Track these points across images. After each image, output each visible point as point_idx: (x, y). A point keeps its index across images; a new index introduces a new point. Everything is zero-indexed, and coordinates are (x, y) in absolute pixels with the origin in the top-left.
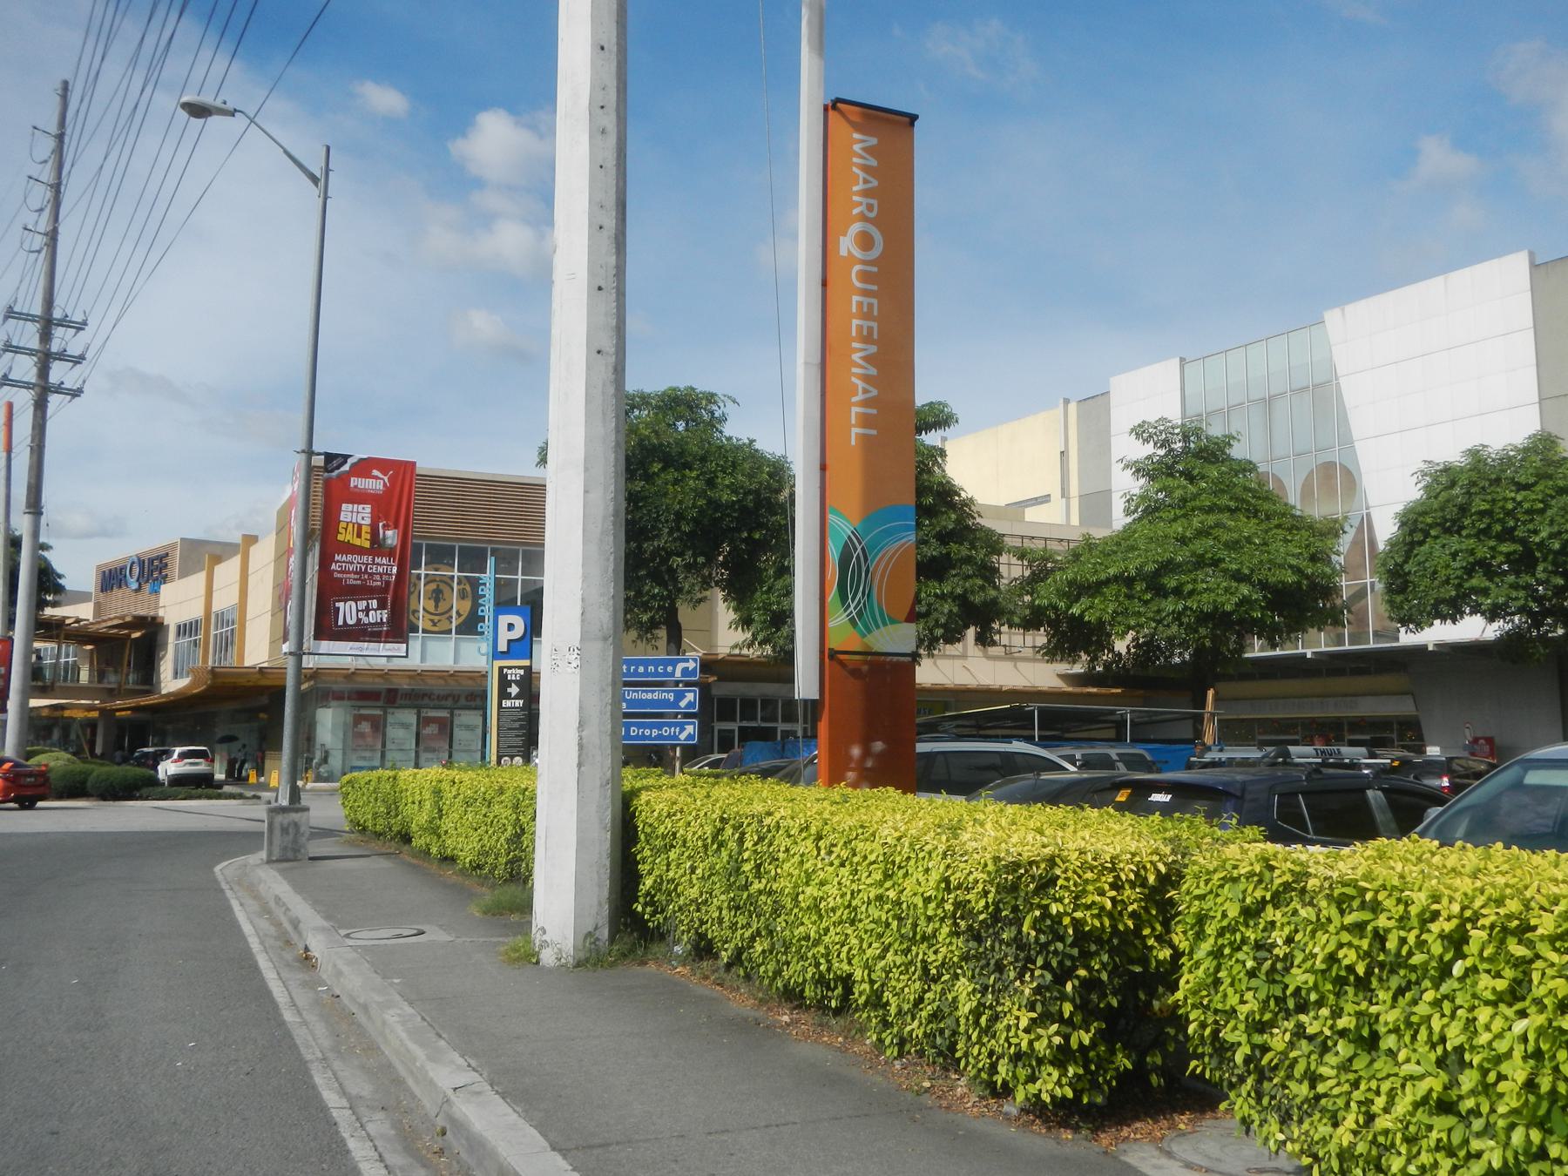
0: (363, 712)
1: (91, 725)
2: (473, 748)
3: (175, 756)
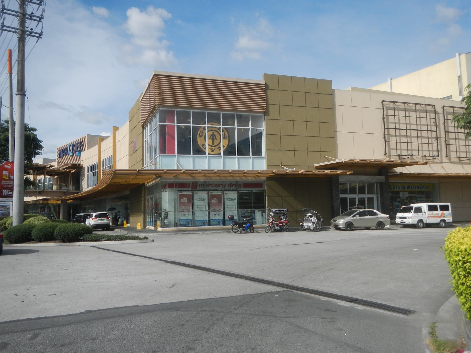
1: (59, 206)
2: (234, 209)
3: (94, 217)
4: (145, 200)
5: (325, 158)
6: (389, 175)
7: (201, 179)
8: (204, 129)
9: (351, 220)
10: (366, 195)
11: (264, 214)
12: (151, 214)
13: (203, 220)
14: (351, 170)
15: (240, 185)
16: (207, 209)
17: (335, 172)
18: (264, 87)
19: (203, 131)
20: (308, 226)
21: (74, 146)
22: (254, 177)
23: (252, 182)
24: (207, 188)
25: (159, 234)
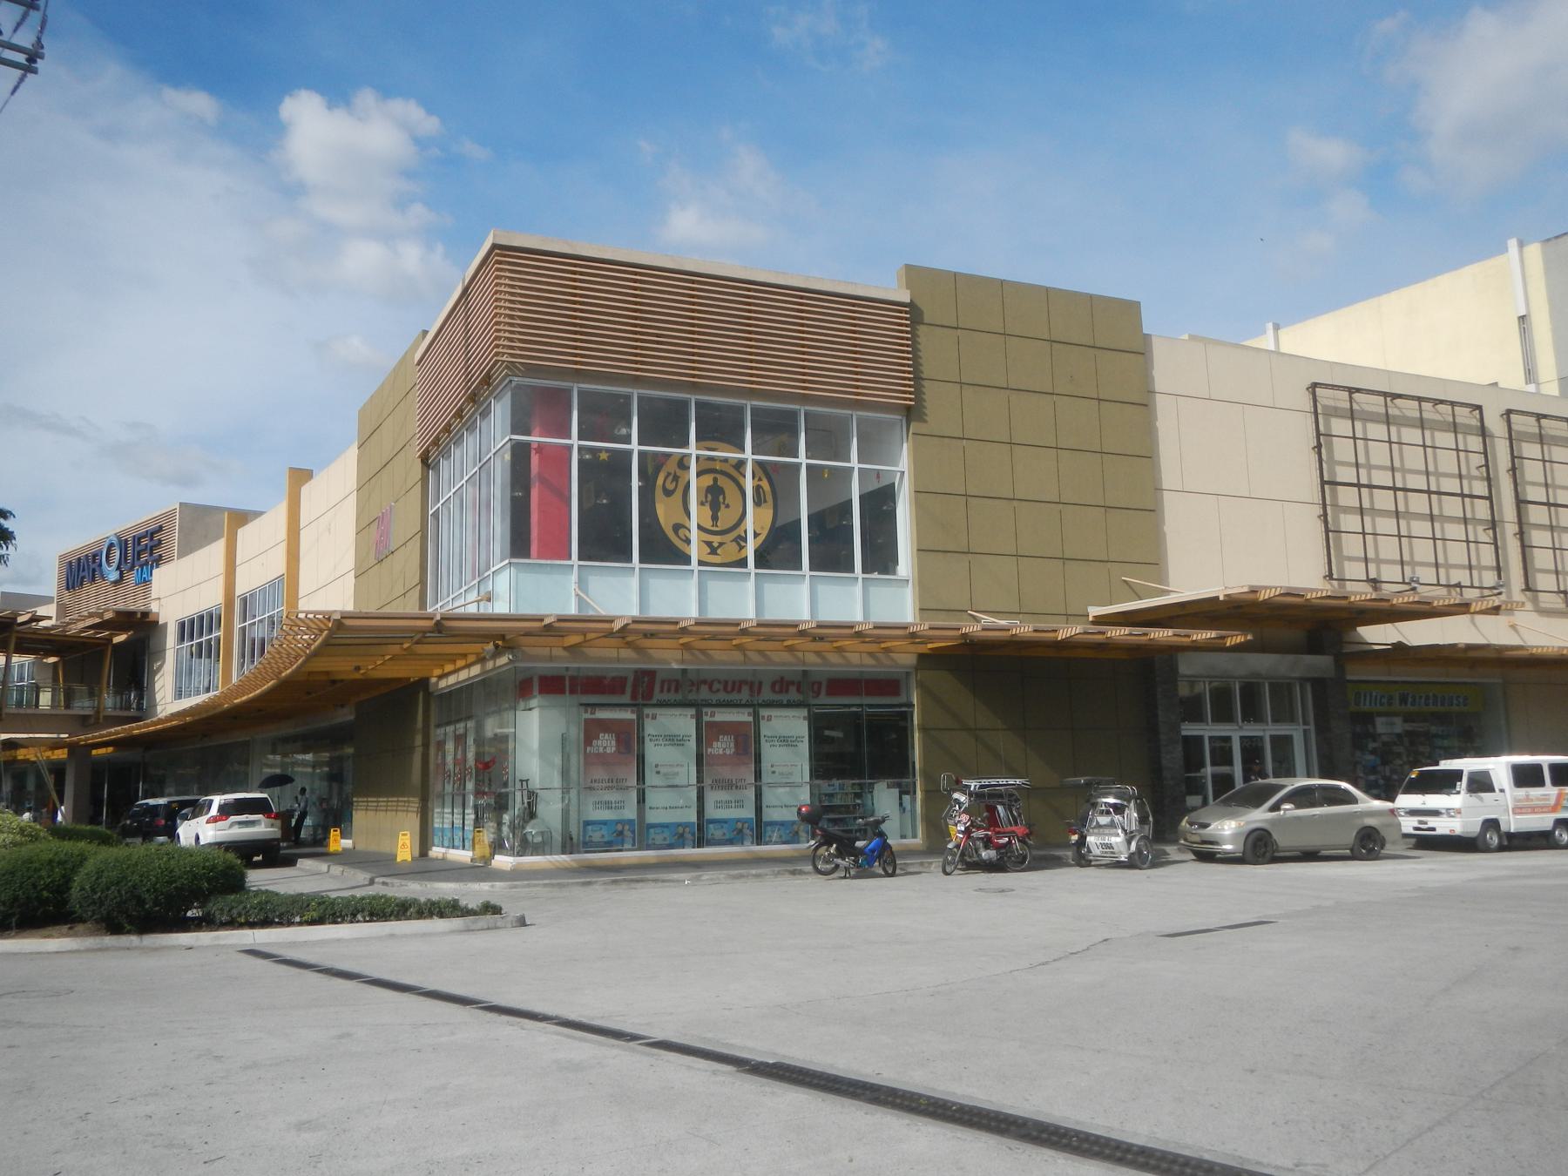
0: (602, 714)
1: (58, 770)
3: (214, 811)
4: (426, 745)
5: (1127, 587)
6: (1344, 651)
7: (669, 658)
8: (683, 464)
9: (1266, 821)
10: (1266, 727)
11: (906, 798)
12: (459, 800)
13: (679, 825)
14: (1243, 629)
15: (816, 687)
16: (694, 780)
17: (1185, 636)
18: (906, 312)
19: (679, 472)
20: (1110, 846)
21: (126, 548)
22: (871, 654)
23: (862, 672)
24: (692, 697)
25: (515, 887)
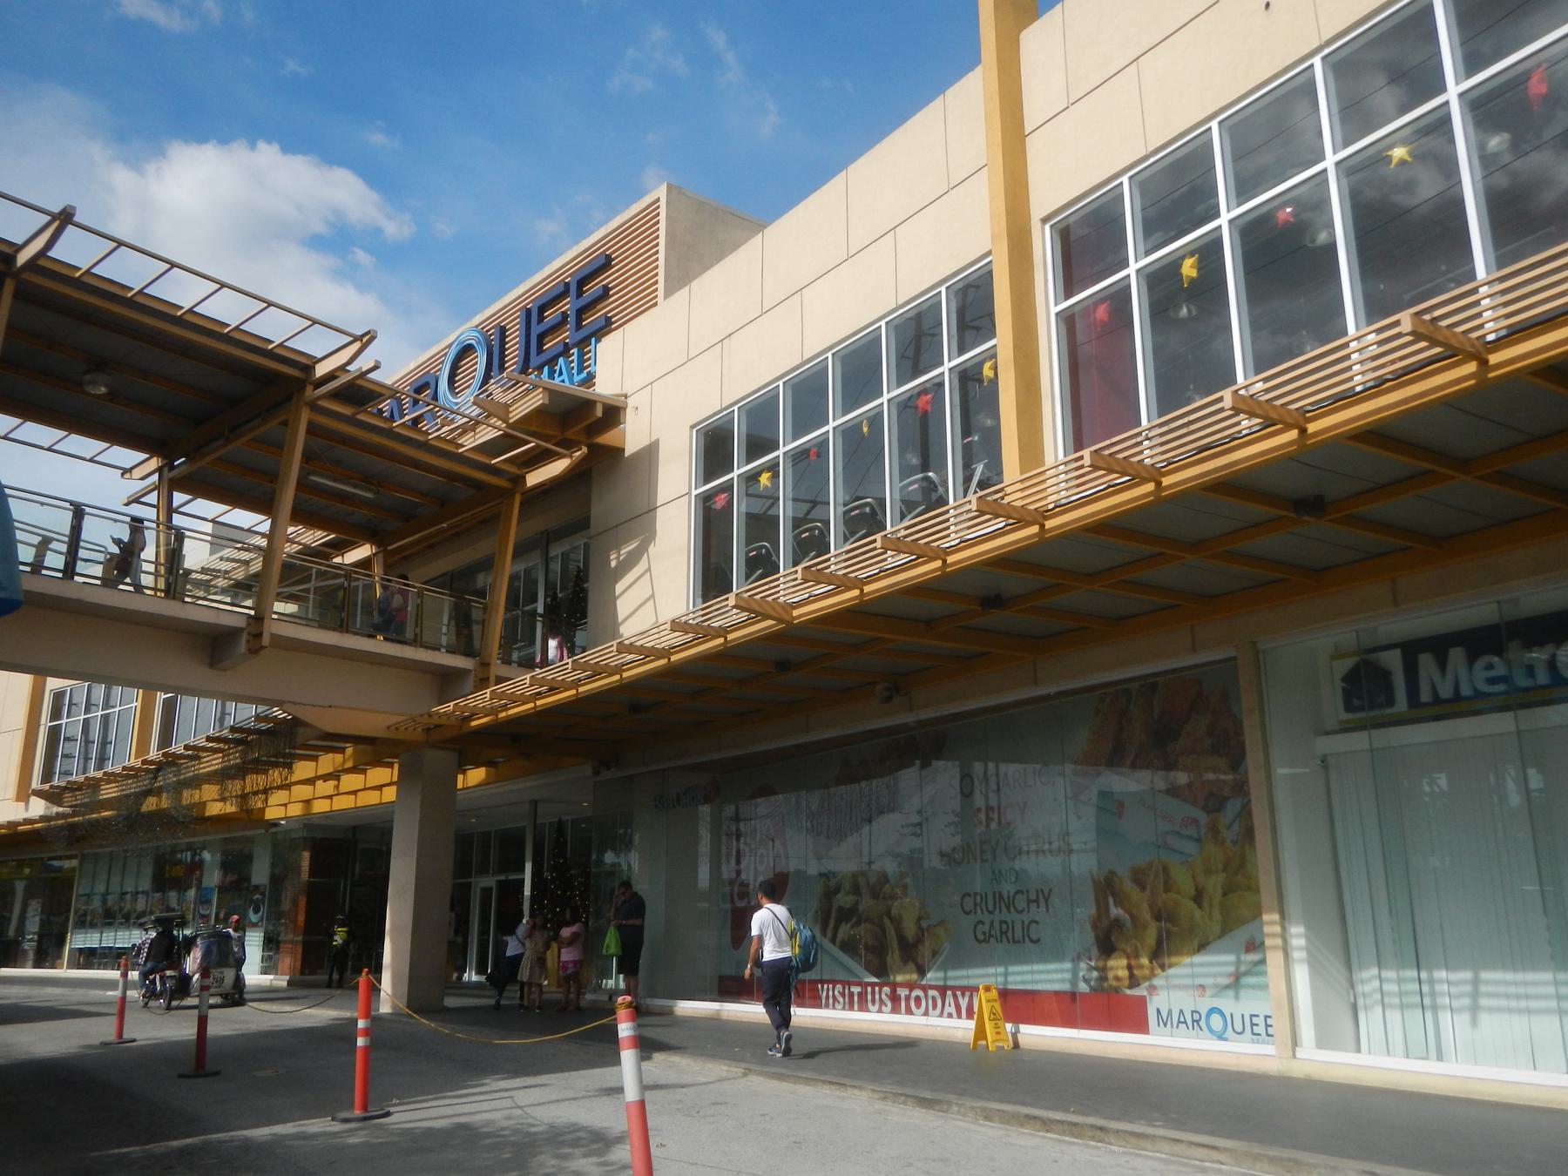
21: (503, 343)
